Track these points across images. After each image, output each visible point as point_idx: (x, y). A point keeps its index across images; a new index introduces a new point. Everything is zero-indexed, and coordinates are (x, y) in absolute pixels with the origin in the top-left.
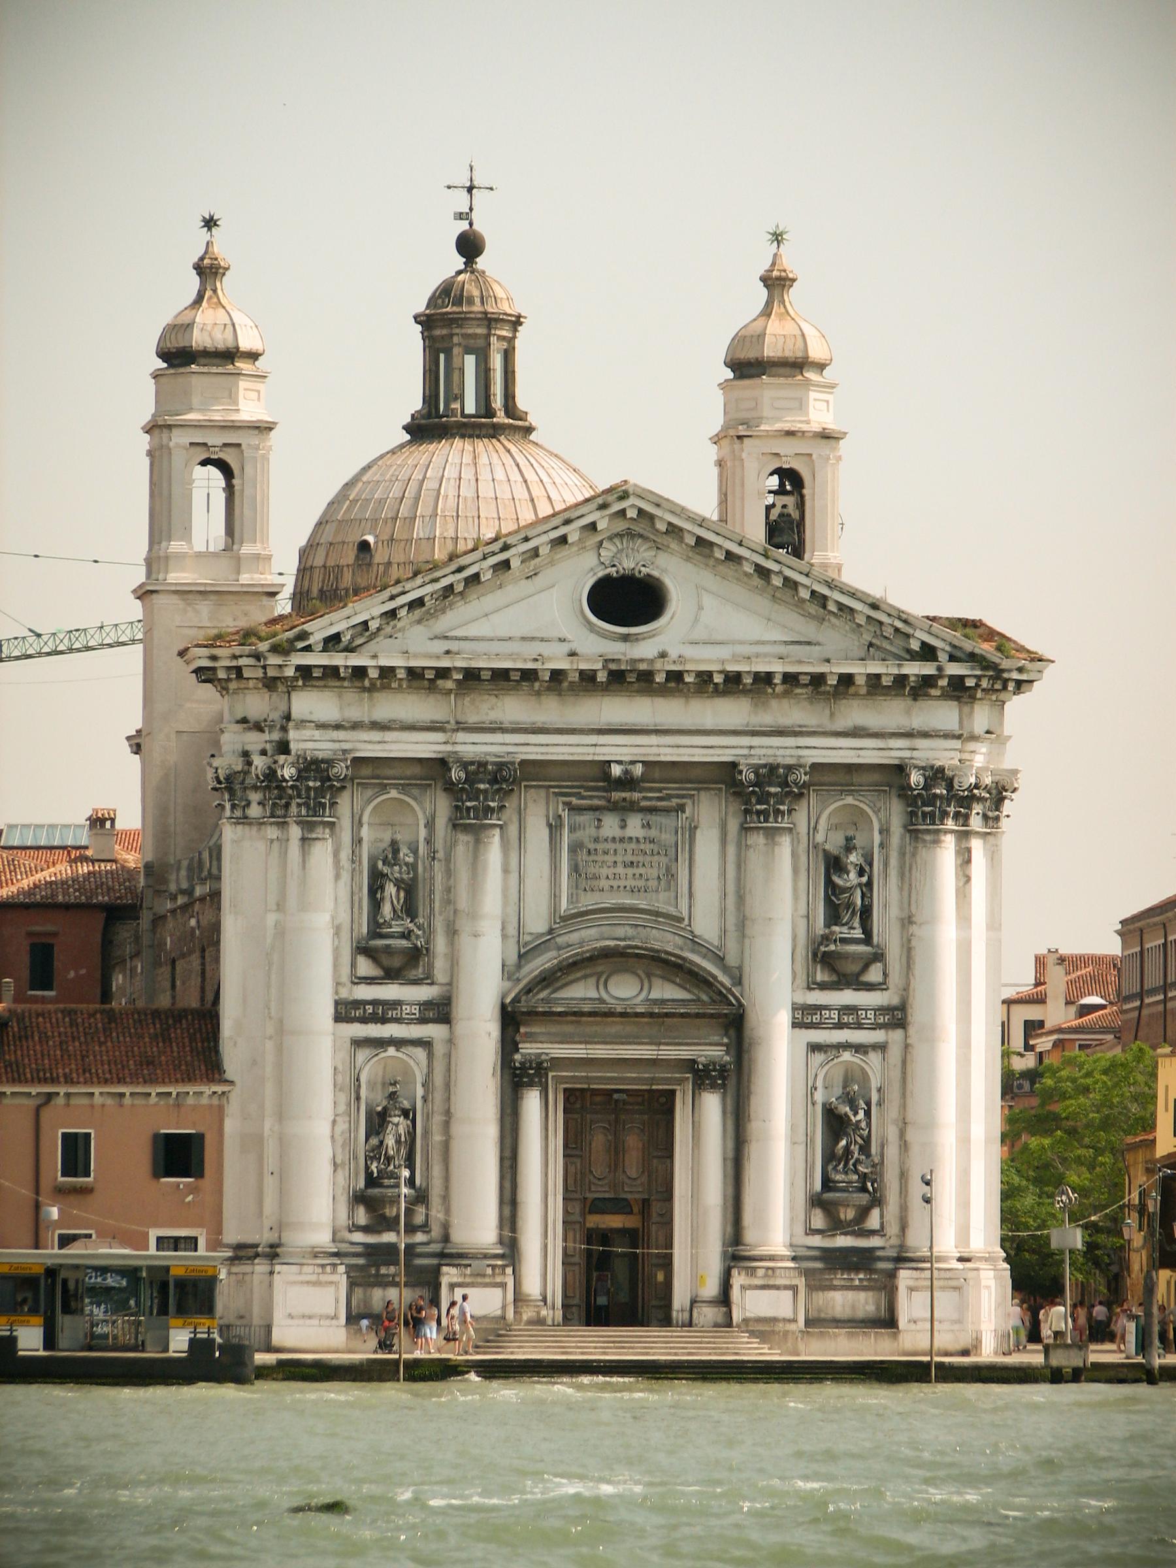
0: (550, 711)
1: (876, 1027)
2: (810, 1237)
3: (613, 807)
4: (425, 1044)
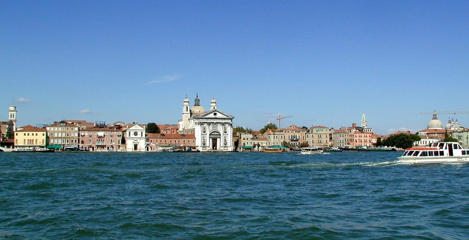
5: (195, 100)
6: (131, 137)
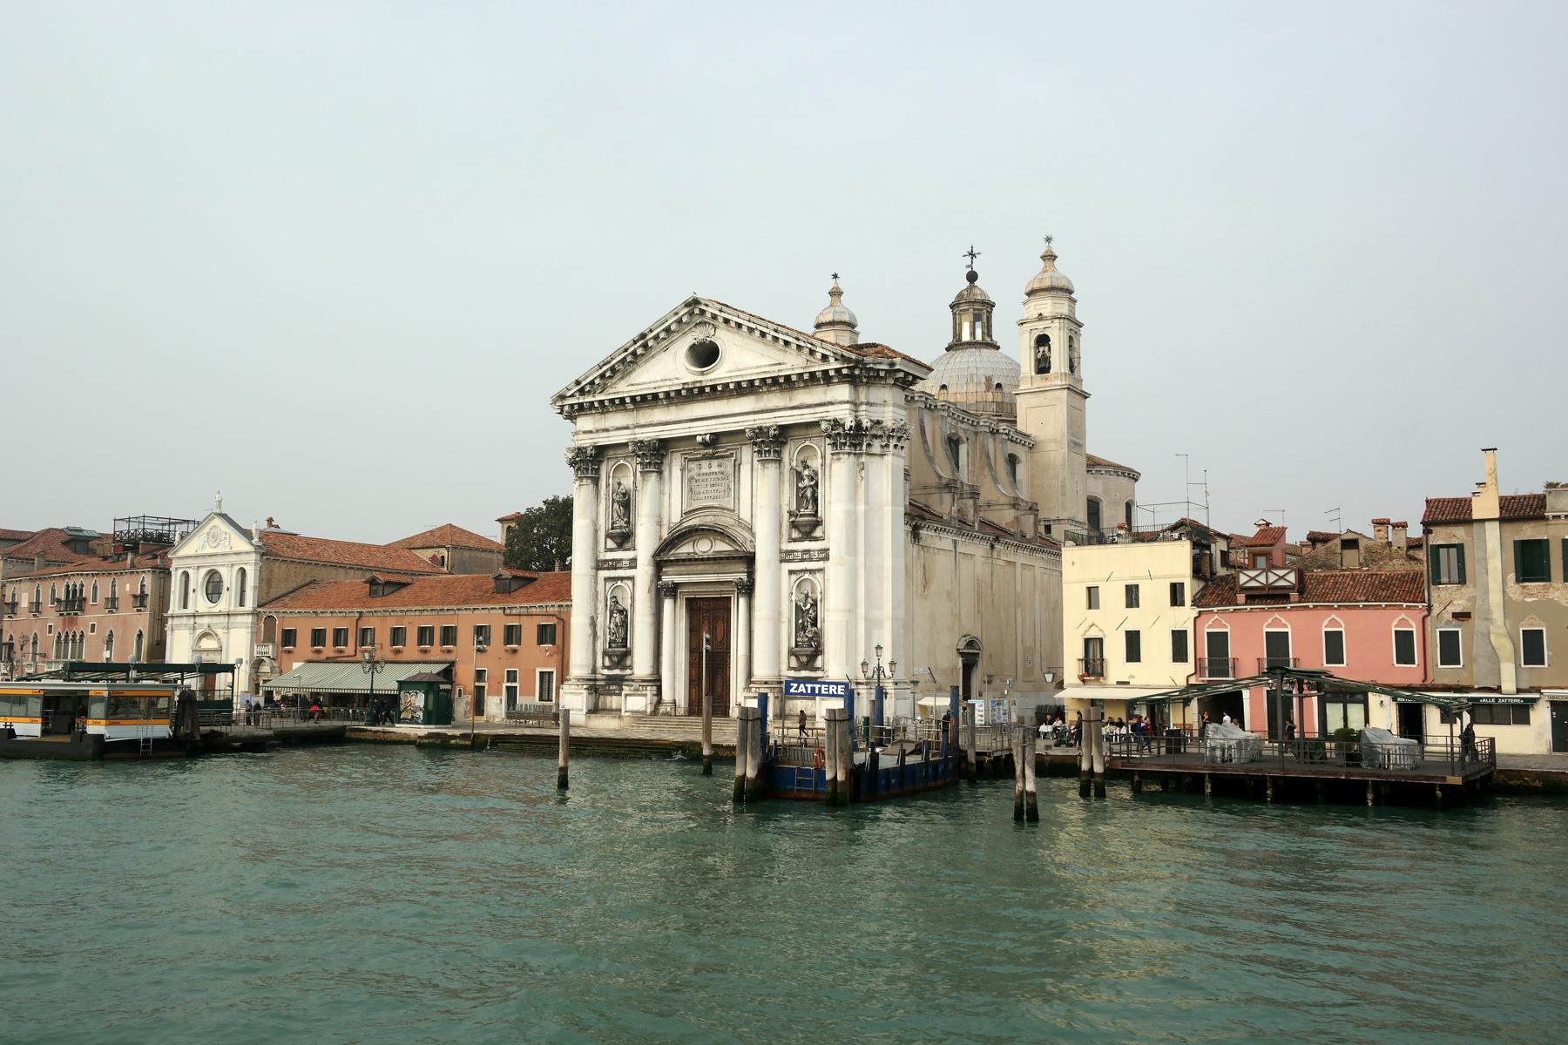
0: (673, 413)
1: (819, 560)
3: (705, 457)
4: (632, 578)
5: (952, 307)
6: (190, 610)
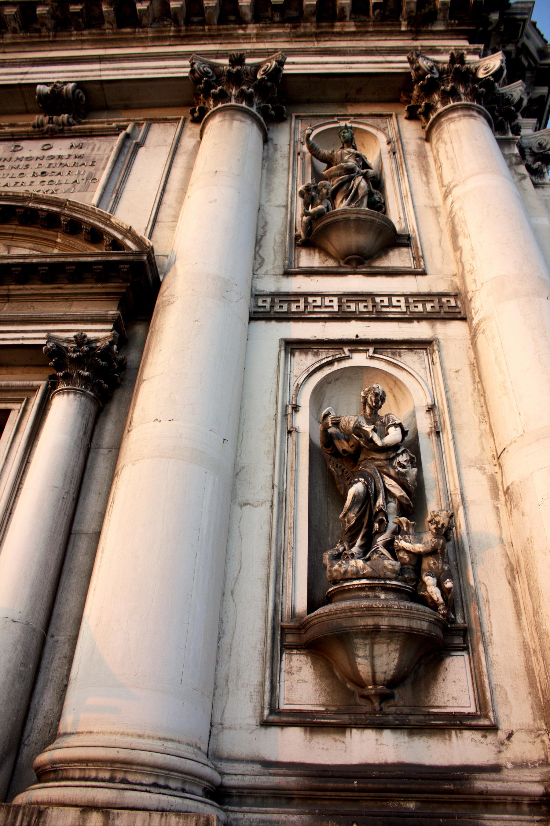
2: (274, 731)
